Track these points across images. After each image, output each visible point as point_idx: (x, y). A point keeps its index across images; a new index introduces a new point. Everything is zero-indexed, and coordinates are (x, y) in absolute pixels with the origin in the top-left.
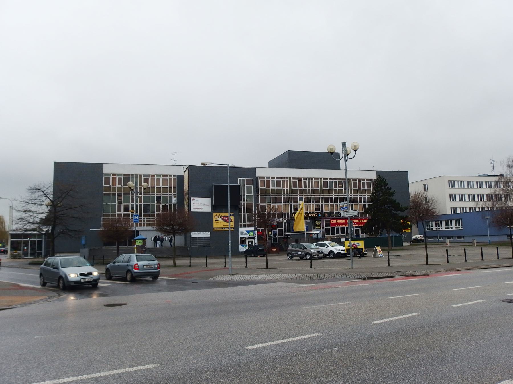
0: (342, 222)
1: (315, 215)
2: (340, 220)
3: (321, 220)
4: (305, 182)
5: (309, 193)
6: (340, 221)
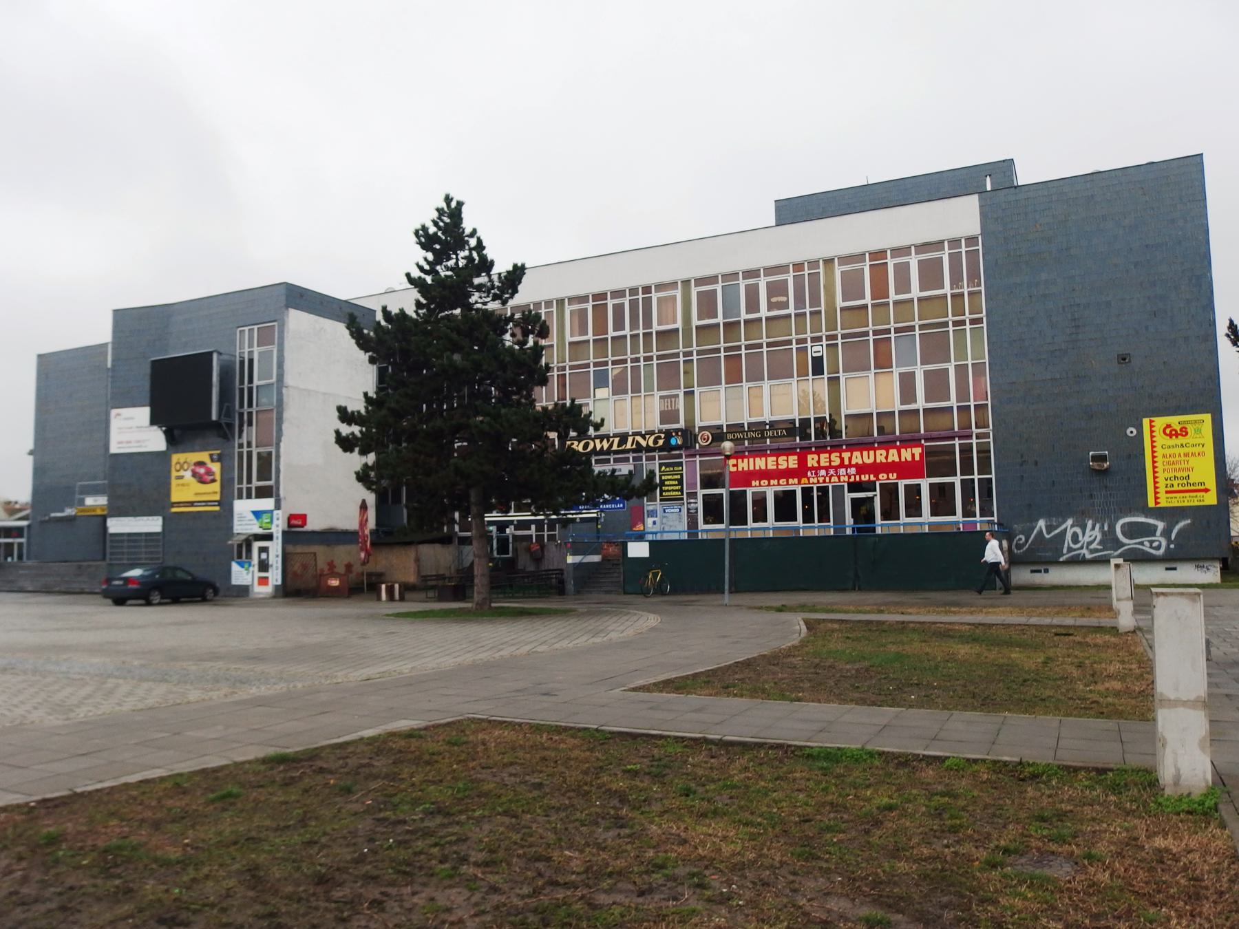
0: (783, 466)
1: (655, 442)
2: (771, 455)
3: (683, 460)
4: (619, 309)
5: (635, 350)
6: (771, 460)
